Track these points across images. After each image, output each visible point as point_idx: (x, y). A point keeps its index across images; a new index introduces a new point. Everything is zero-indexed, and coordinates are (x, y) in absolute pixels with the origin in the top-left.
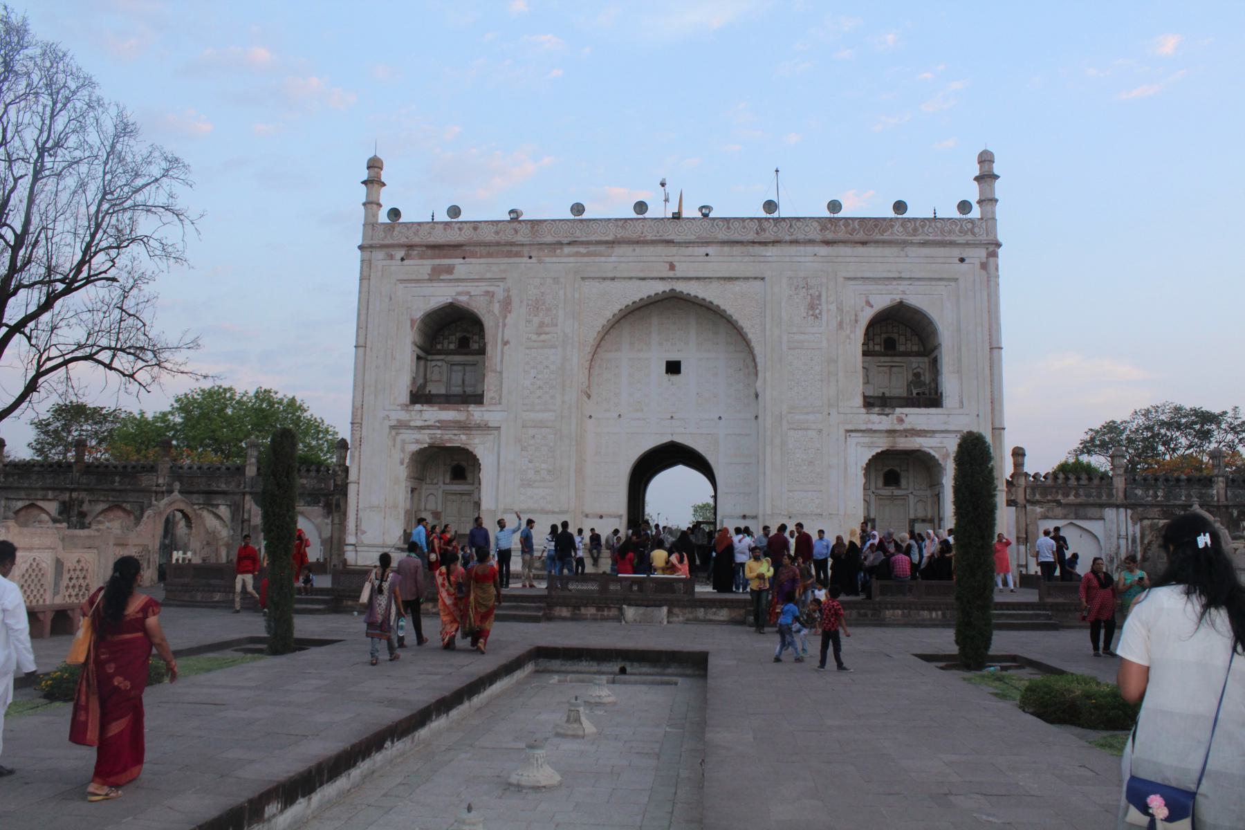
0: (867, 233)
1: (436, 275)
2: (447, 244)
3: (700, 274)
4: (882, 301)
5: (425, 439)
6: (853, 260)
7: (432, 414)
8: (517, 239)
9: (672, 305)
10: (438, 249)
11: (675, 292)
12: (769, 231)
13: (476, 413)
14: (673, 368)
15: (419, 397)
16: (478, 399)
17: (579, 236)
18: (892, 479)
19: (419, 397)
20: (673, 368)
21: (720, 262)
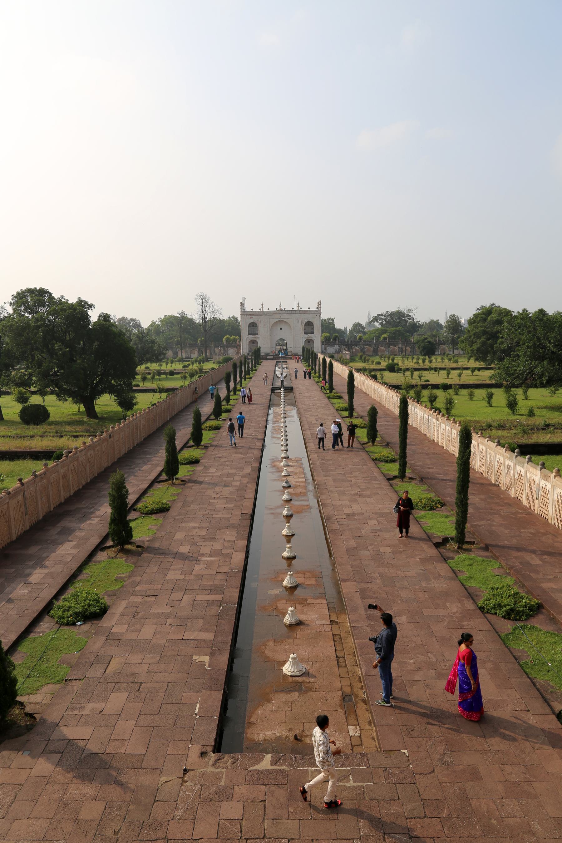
0: (305, 312)
1: (251, 318)
2: (252, 314)
3: (284, 317)
4: (307, 321)
5: (251, 339)
6: (303, 316)
7: (251, 336)
8: (261, 313)
9: (281, 321)
10: (250, 315)
11: (280, 318)
12: (292, 312)
13: (257, 336)
14: (281, 329)
15: (249, 334)
16: (257, 334)
17: (269, 313)
18: (309, 342)
19: (249, 334)
20: (281, 329)
21: (287, 316)
